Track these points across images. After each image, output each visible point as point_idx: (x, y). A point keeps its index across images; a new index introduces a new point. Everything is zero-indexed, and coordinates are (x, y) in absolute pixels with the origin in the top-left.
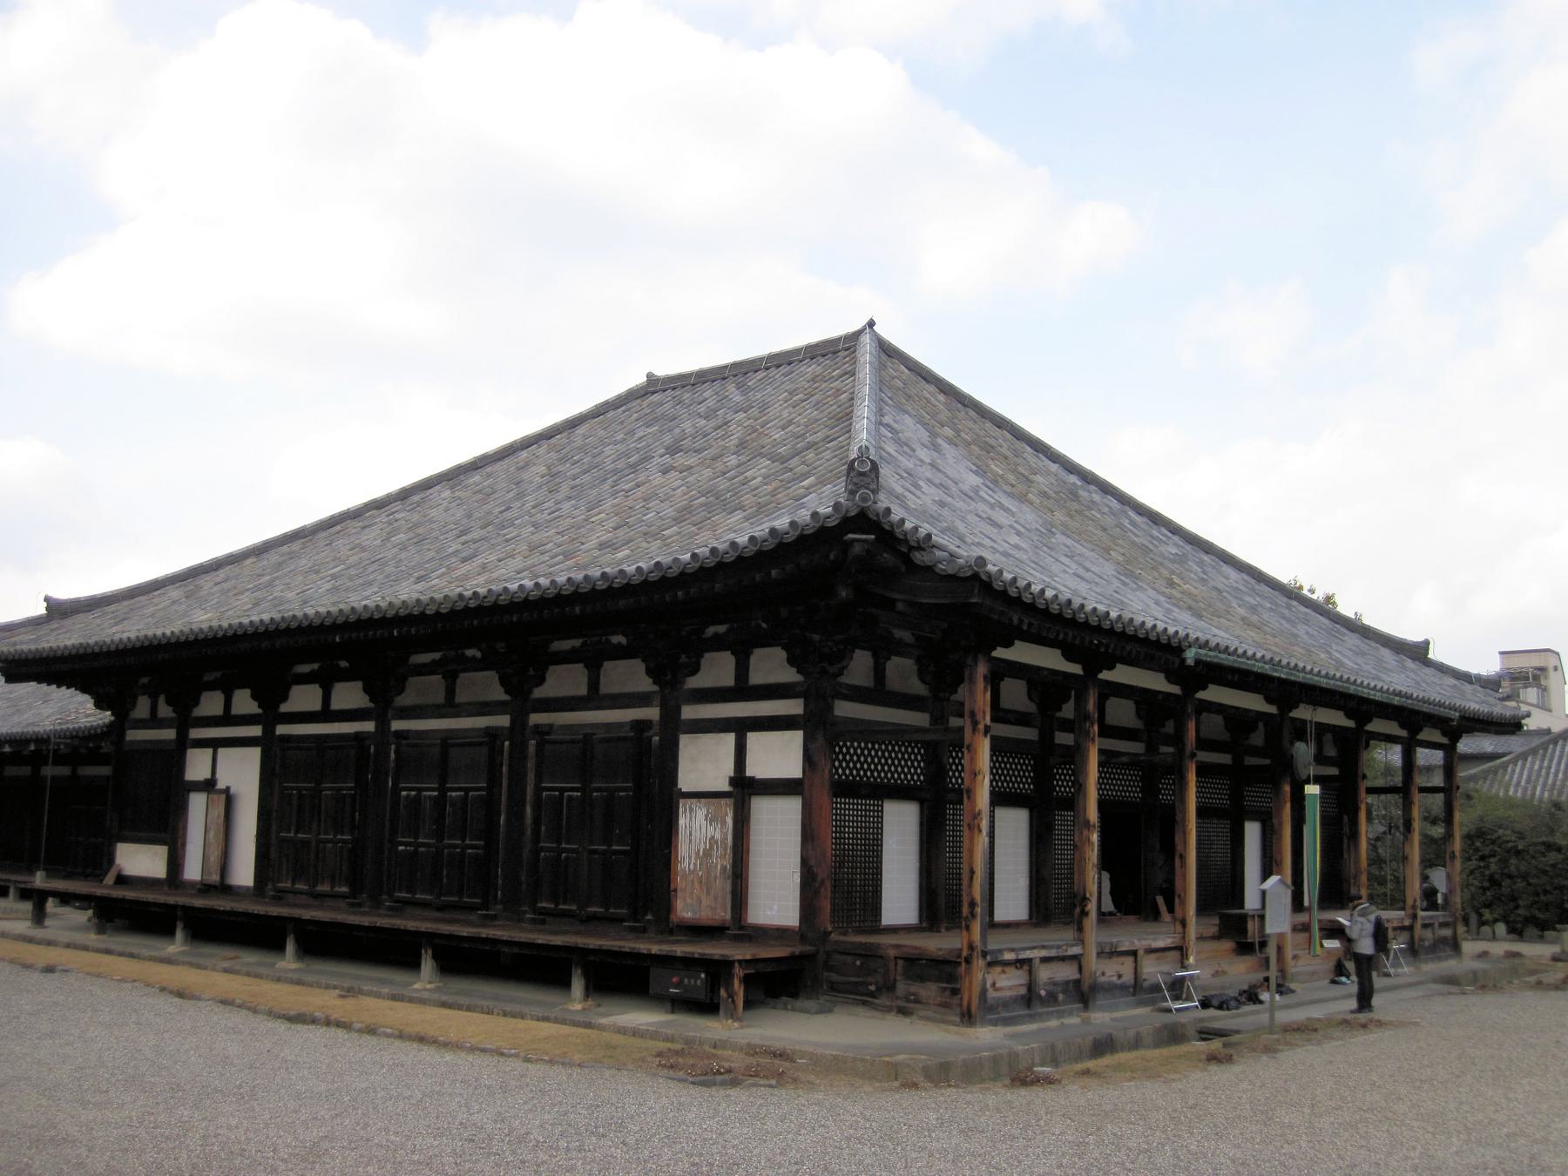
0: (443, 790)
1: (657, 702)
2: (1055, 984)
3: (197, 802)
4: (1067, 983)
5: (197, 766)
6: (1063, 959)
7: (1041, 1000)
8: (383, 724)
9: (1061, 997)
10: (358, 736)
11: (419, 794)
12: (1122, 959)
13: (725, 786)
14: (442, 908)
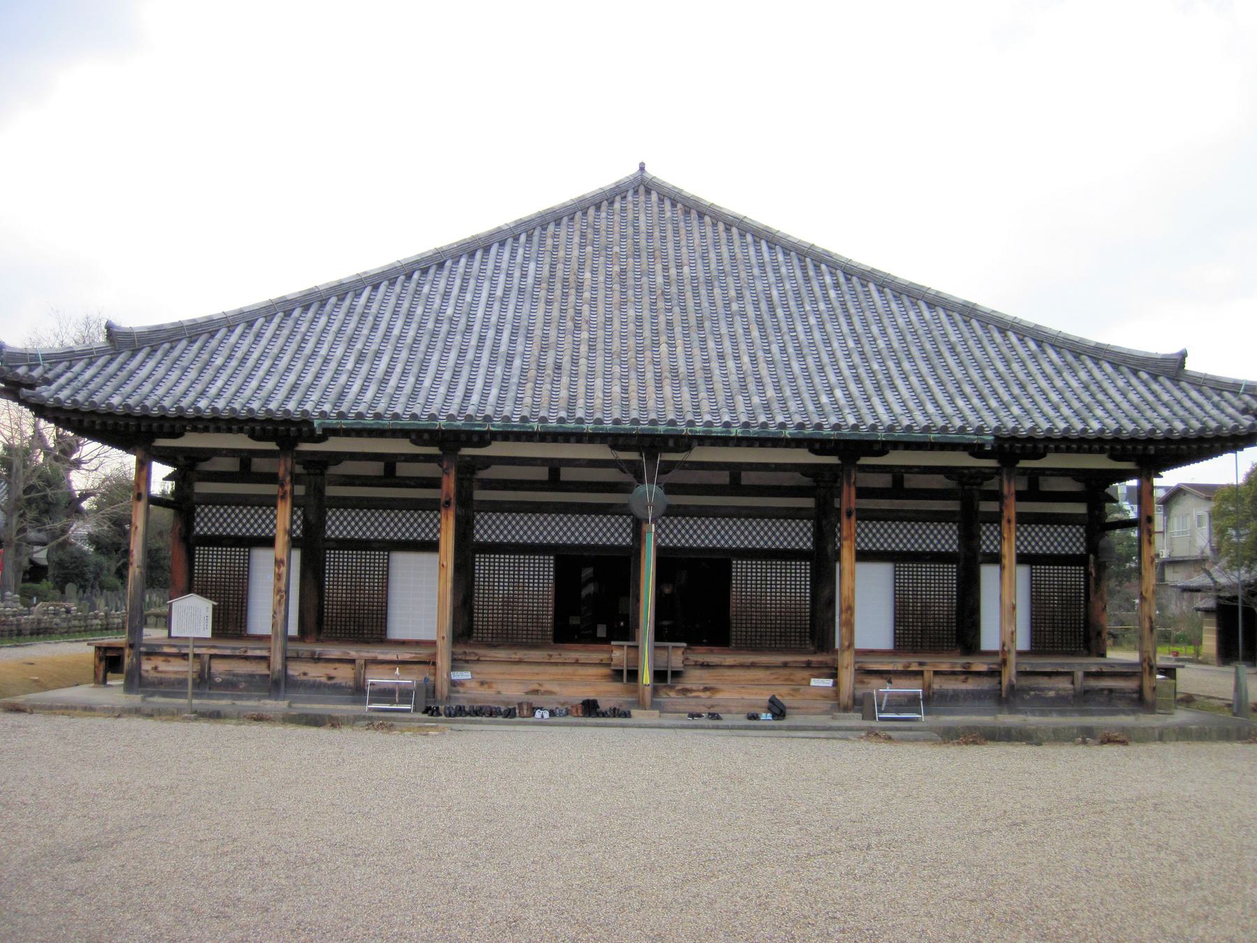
2: (234, 675)
4: (252, 676)
6: (247, 658)
7: (219, 686)
9: (242, 685)
12: (337, 665)
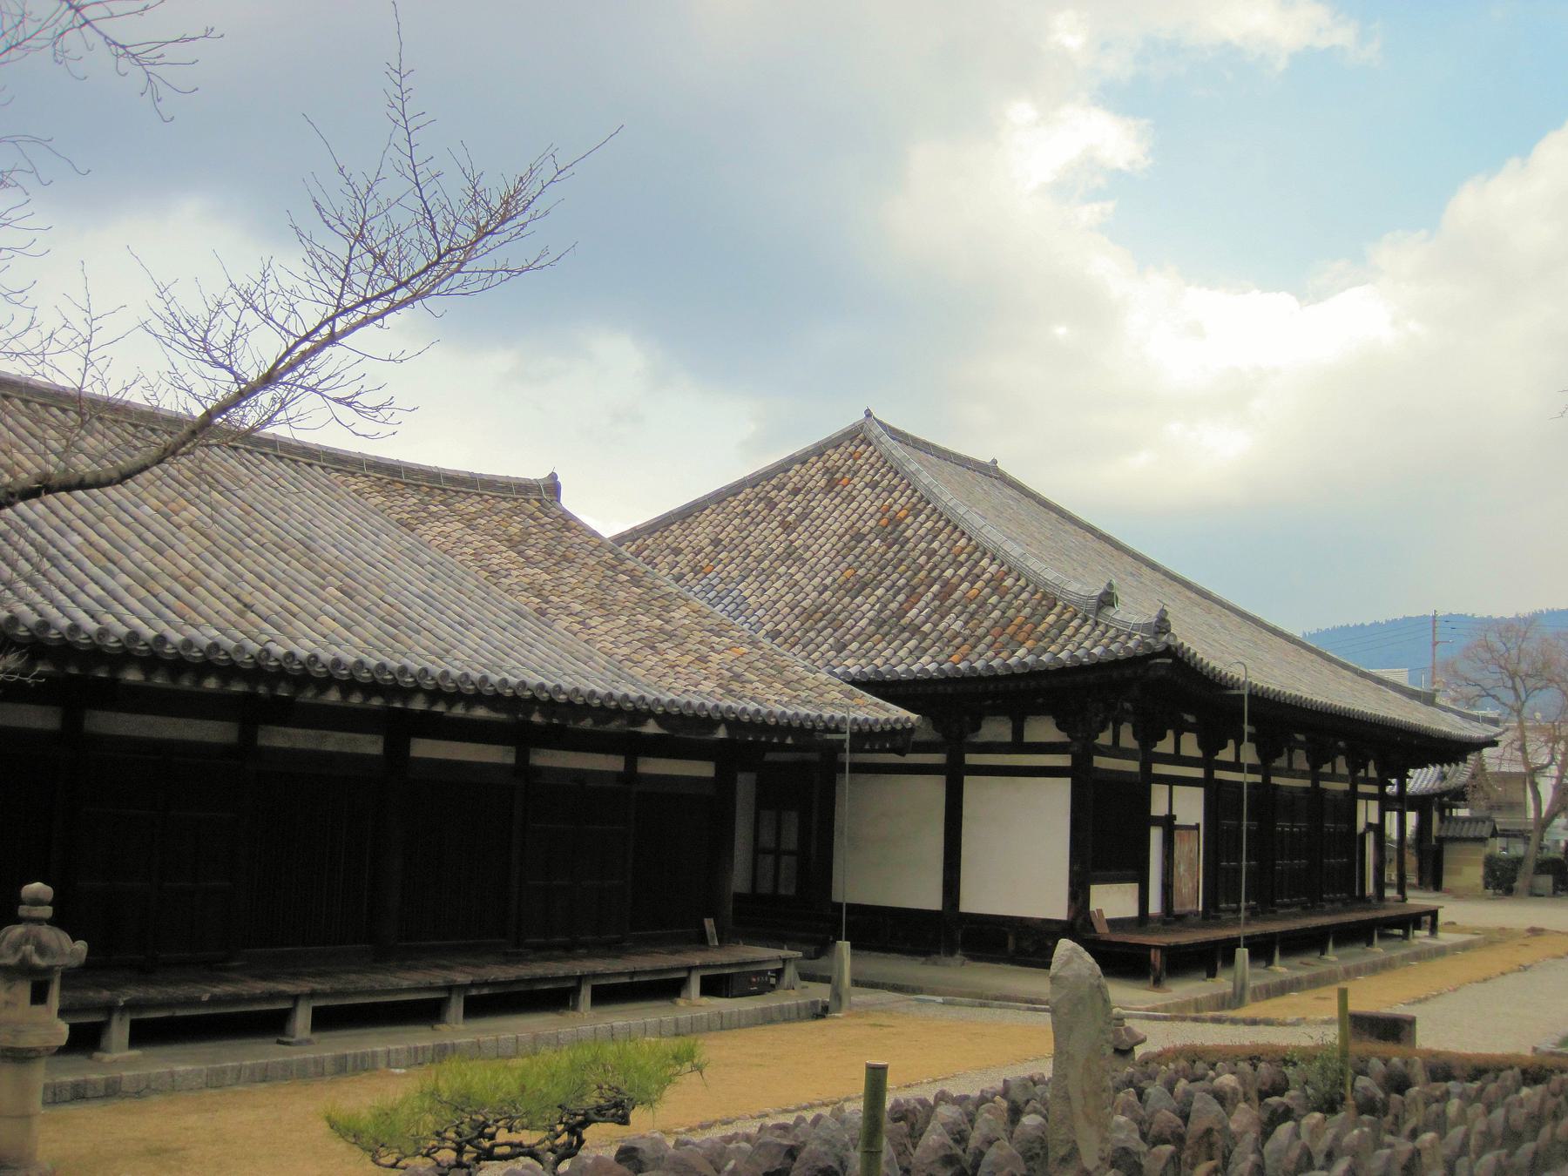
3: (1156, 834)
8: (1266, 779)
14: (1287, 906)
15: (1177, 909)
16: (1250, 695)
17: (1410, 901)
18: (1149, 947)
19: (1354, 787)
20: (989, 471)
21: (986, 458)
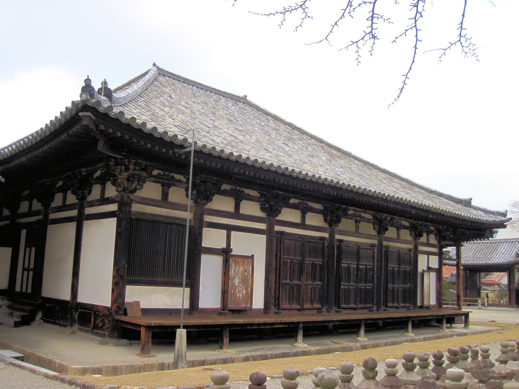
0: (358, 265)
1: (413, 244)
5: (212, 238)
8: (332, 236)
10: (322, 239)
11: (349, 267)
13: (425, 269)
15: (231, 305)
16: (195, 151)
17: (462, 310)
18: (140, 326)
19: (416, 247)
20: (243, 100)
21: (241, 95)
